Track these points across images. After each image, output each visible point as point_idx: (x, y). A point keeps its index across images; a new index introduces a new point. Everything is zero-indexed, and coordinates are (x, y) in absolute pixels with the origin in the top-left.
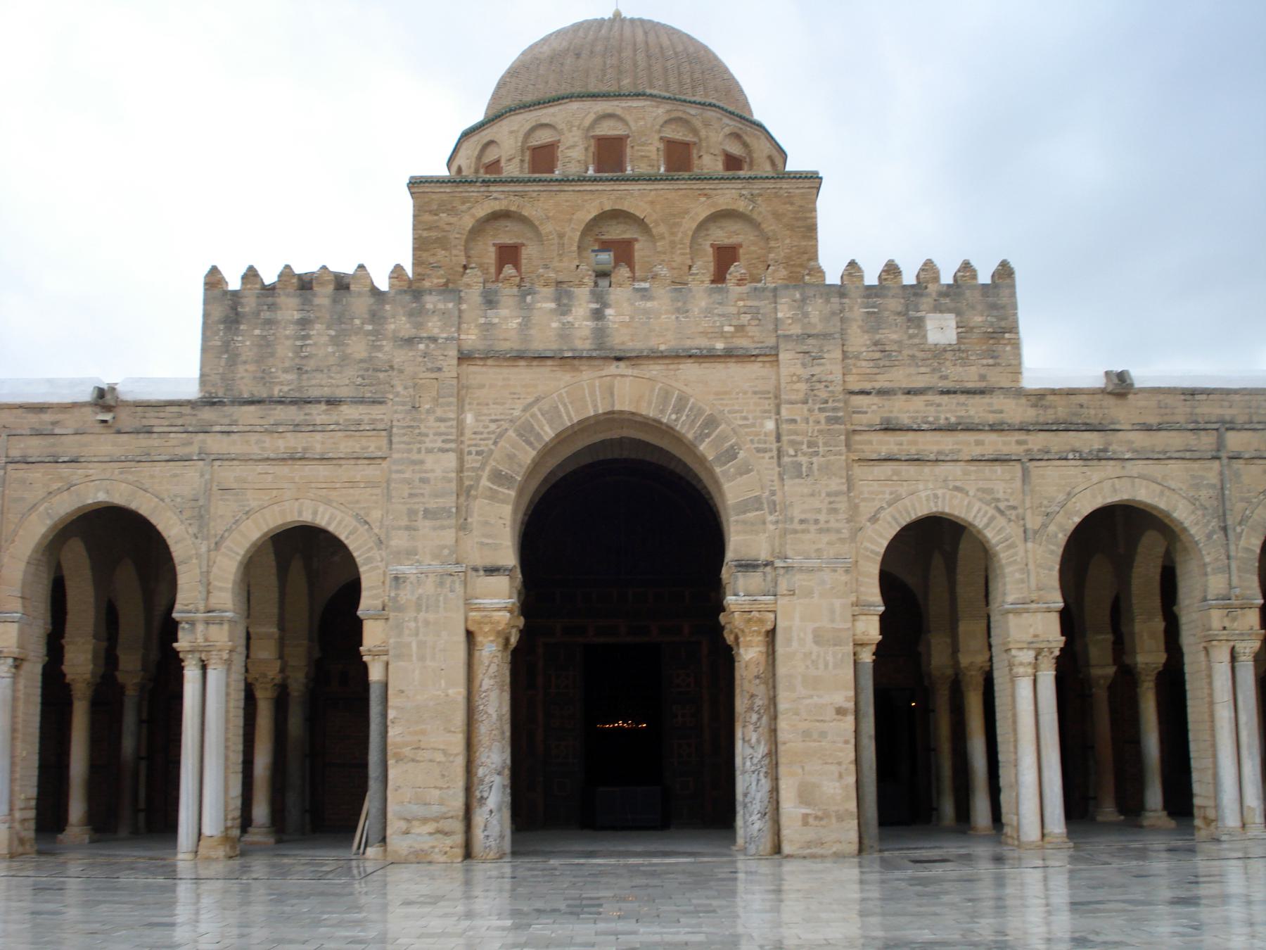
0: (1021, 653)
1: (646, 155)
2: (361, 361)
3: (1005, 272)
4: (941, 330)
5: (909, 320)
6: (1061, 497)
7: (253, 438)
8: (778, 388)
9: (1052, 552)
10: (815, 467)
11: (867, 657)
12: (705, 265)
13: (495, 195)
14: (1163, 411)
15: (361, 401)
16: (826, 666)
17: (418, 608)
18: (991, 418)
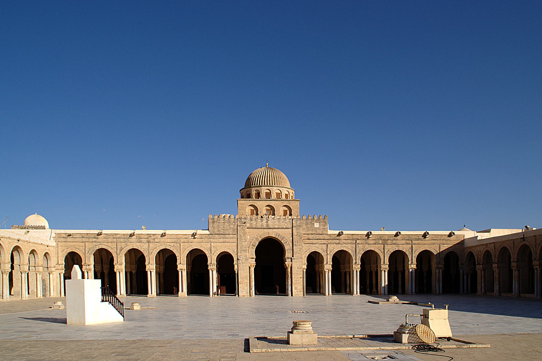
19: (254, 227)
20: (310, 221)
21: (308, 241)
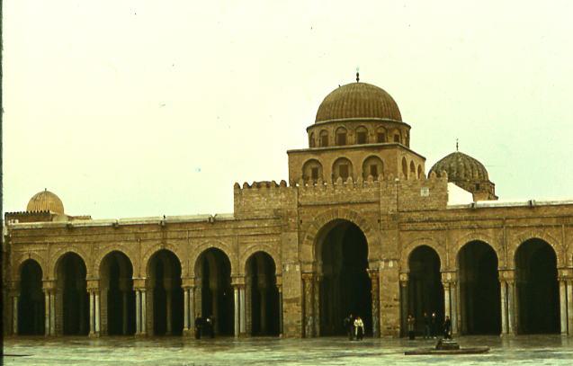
18: (438, 218)
21: (410, 226)
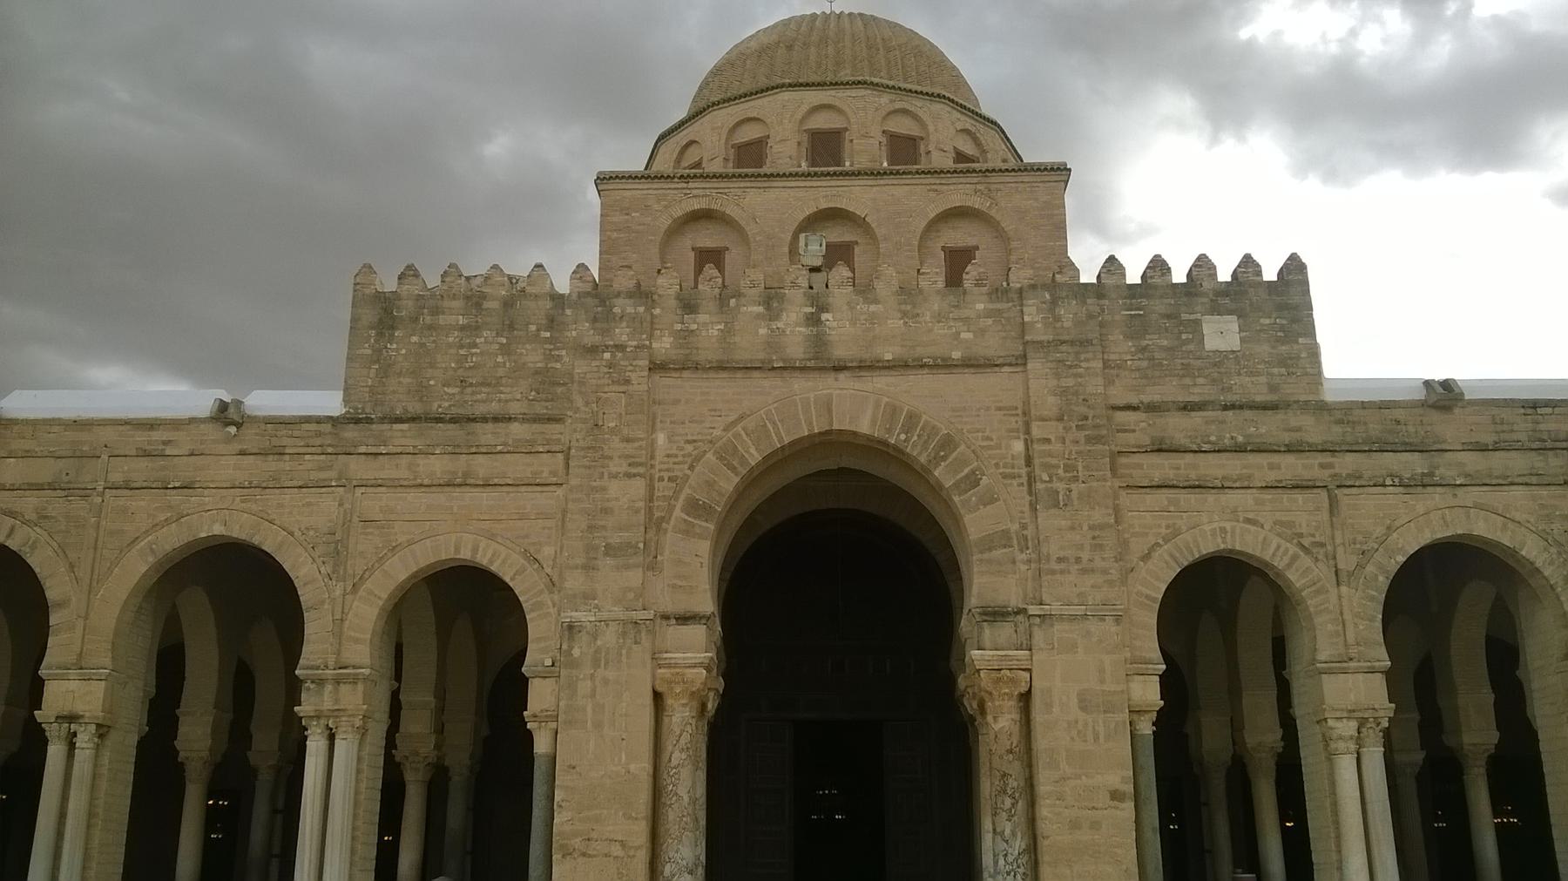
0: (1338, 724)
1: (865, 149)
2: (537, 372)
3: (1294, 269)
4: (1221, 334)
5: (1181, 323)
6: (1380, 531)
7: (405, 460)
8: (1026, 402)
9: (1372, 599)
10: (1074, 494)
11: (1146, 728)
12: (935, 274)
13: (695, 192)
14: (1499, 428)
15: (537, 419)
16: (1096, 738)
17: (596, 663)
18: (1287, 438)
19: (708, 350)
20: (1159, 306)
